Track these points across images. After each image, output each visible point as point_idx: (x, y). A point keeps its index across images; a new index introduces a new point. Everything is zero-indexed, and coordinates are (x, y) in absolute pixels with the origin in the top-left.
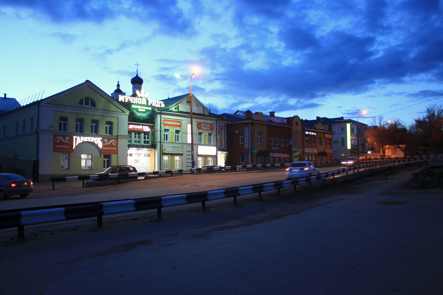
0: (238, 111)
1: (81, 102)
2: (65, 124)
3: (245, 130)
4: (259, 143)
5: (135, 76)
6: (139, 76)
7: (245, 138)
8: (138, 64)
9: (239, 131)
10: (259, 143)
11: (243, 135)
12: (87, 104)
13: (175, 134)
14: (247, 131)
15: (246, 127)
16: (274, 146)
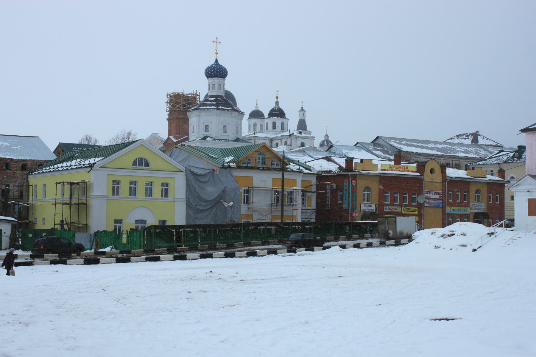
0: (378, 138)
1: (134, 164)
2: (118, 188)
3: (345, 184)
4: (366, 202)
5: (213, 62)
6: (220, 62)
7: (344, 194)
8: (219, 40)
9: (337, 186)
10: (366, 202)
11: (342, 191)
12: (141, 164)
13: (243, 194)
14: (346, 186)
15: (346, 180)
16: (392, 204)
